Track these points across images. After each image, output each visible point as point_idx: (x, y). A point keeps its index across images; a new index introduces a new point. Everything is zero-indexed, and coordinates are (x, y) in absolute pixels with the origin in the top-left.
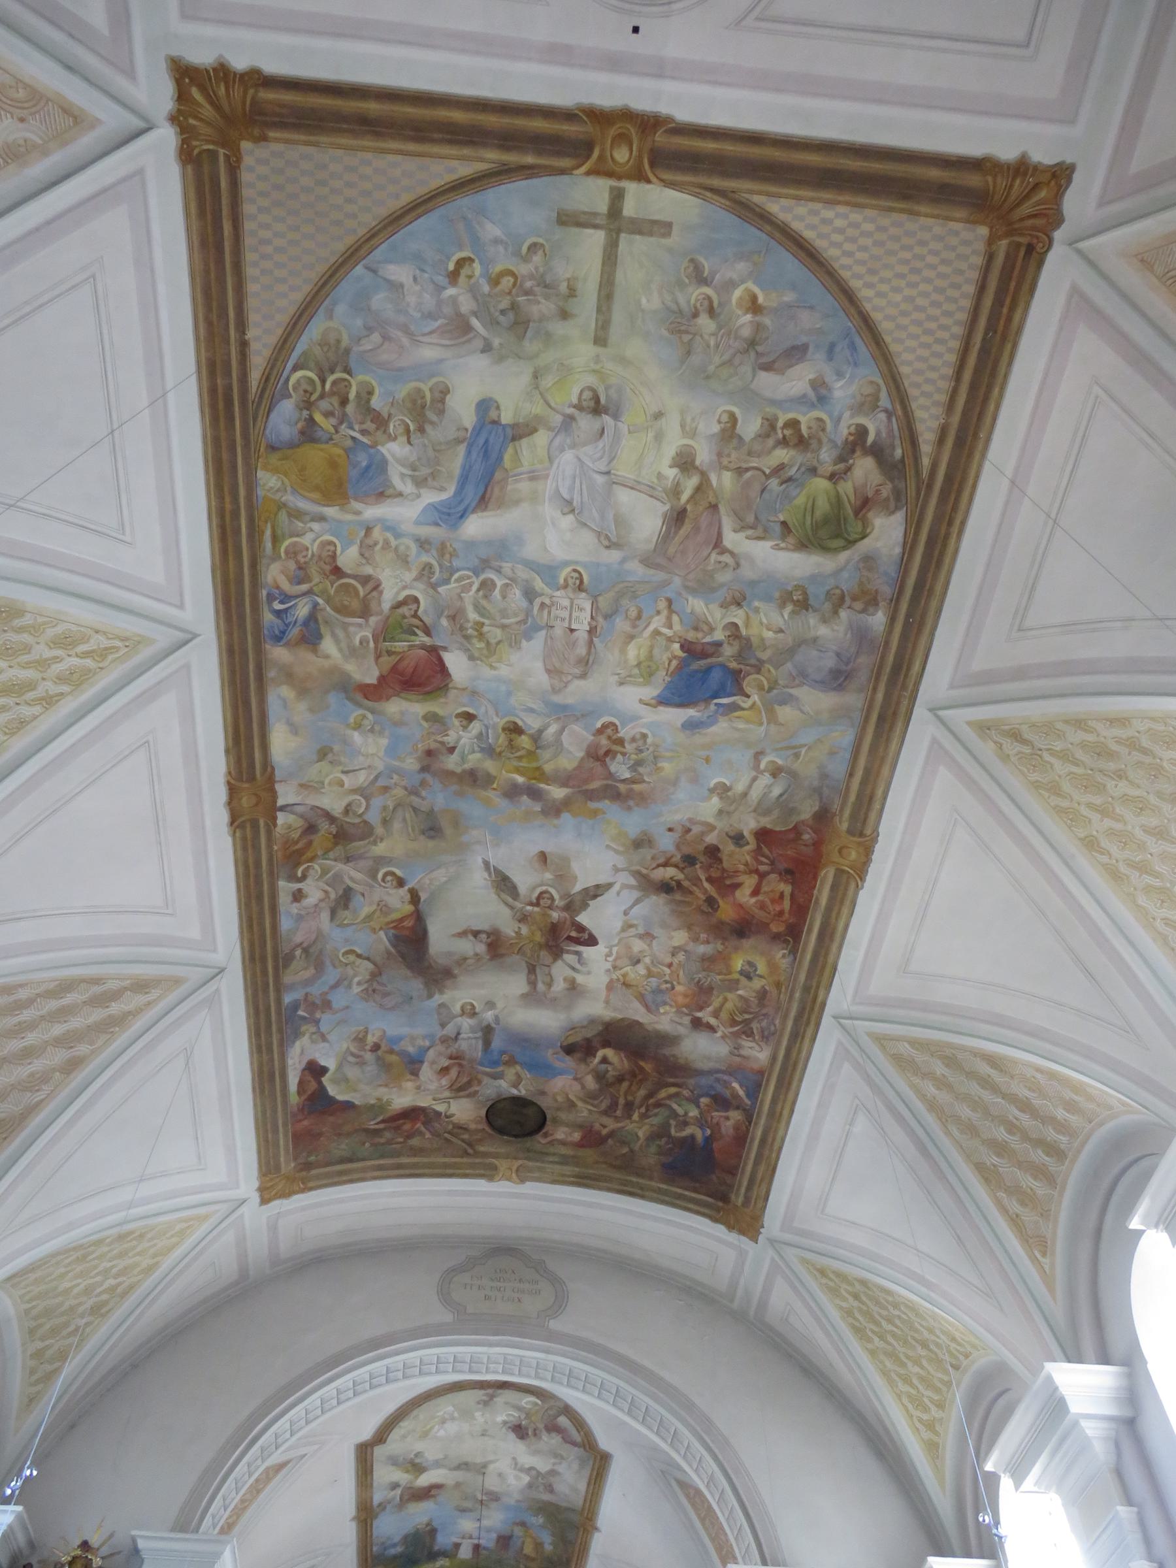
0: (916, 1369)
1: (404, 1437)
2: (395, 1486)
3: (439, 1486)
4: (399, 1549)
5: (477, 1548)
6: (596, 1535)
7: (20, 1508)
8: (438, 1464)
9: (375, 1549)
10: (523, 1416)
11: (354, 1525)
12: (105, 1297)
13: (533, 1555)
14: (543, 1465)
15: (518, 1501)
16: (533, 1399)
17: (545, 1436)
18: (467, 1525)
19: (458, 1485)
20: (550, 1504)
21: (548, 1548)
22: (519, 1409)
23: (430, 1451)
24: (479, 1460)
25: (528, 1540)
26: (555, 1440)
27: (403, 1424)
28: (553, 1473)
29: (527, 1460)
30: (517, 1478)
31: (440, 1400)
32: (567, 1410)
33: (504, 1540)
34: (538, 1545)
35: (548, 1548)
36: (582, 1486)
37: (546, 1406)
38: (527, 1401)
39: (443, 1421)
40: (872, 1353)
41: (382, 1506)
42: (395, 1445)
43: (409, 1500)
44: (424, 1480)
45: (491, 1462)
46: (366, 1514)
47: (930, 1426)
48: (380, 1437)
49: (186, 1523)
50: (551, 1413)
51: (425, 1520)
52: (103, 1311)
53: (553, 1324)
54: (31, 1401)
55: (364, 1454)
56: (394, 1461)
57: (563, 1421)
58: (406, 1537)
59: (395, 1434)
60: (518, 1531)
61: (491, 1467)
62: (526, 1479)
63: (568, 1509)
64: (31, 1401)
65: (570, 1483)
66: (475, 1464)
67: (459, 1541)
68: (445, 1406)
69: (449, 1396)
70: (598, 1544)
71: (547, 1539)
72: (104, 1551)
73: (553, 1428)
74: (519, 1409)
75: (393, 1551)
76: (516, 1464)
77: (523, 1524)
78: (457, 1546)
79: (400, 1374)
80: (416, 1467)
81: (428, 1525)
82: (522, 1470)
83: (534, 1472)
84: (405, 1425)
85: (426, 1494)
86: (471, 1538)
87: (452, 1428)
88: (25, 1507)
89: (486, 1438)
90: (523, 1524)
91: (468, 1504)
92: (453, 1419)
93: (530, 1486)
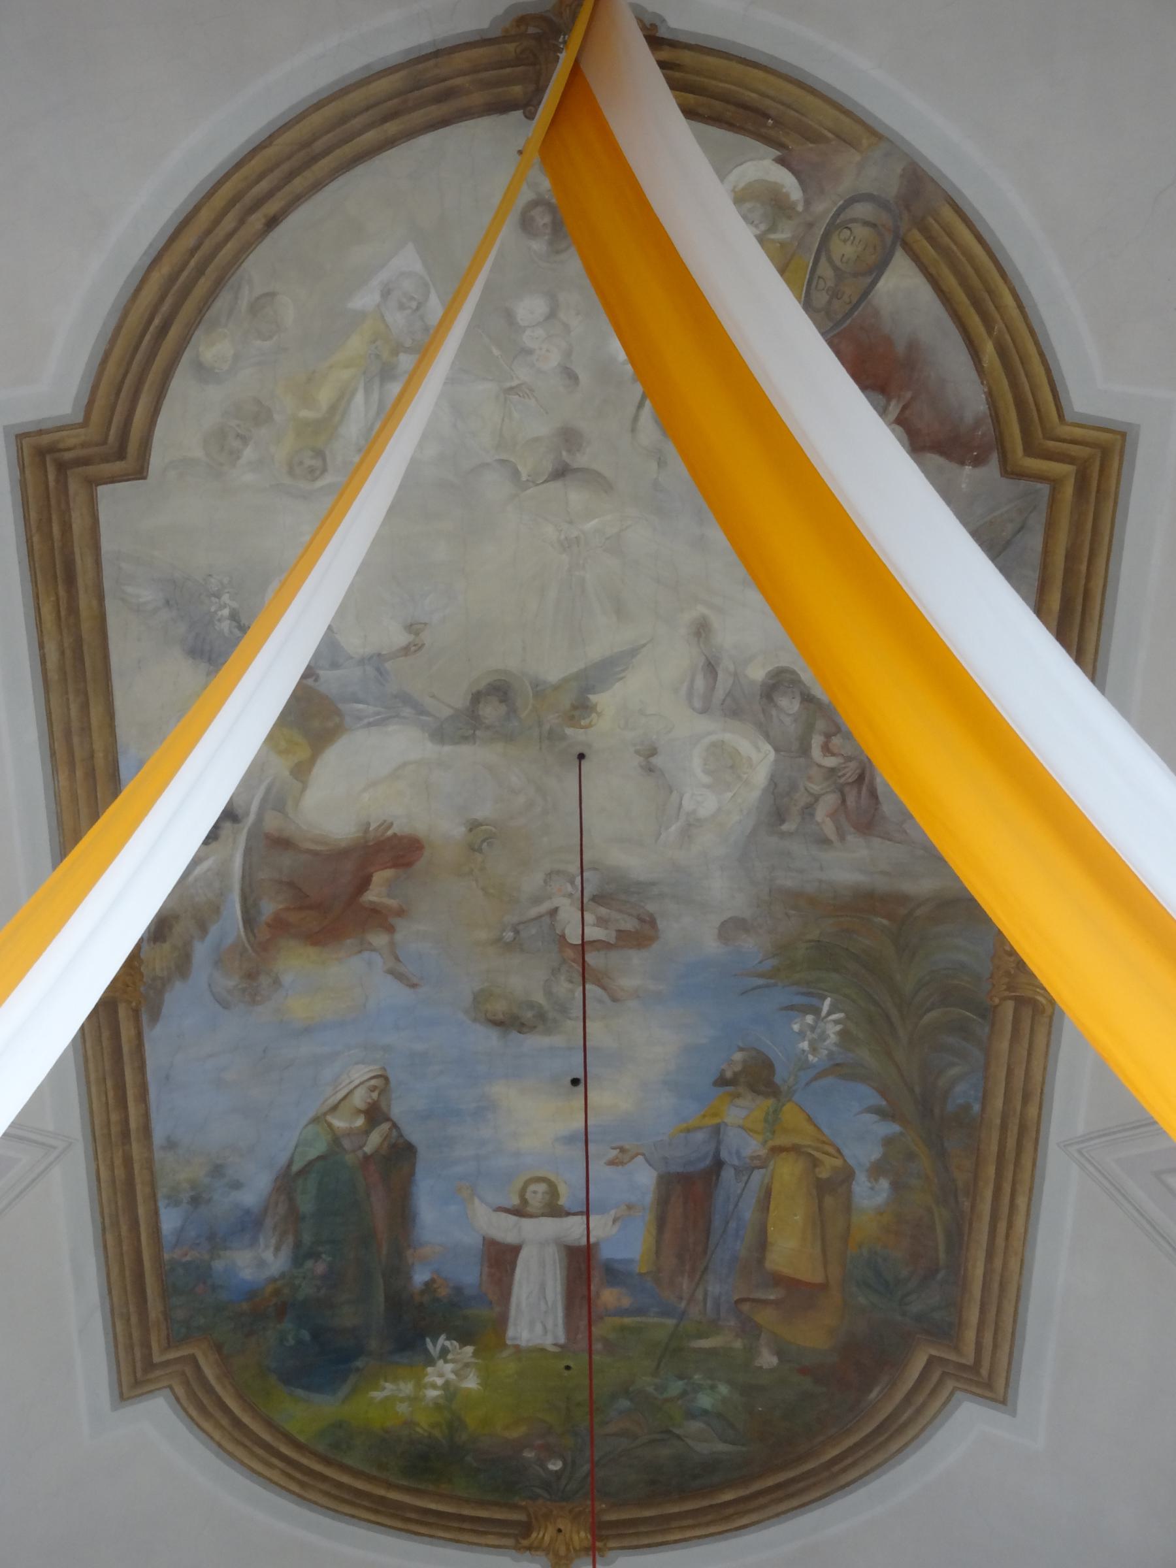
1: (225, 443)
4: (259, 1263)
5: (581, 1263)
9: (170, 1220)
13: (808, 1271)
15: (731, 928)
18: (532, 1123)
19: (481, 838)
20: (866, 904)
21: (870, 1195)
24: (554, 667)
25: (787, 1172)
27: (214, 347)
30: (725, 764)
31: (361, 193)
33: (691, 1194)
34: (830, 1188)
35: (870, 1195)
37: (825, 207)
45: (606, 671)
50: (844, 249)
58: (288, 1182)
59: (184, 423)
61: (605, 700)
66: (540, 690)
67: (506, 1229)
69: (398, 163)
76: (711, 668)
78: (501, 1259)
81: (374, 1114)
82: (734, 710)
83: (789, 704)
86: (554, 1210)
89: (576, 496)
91: (526, 980)
93: (779, 808)
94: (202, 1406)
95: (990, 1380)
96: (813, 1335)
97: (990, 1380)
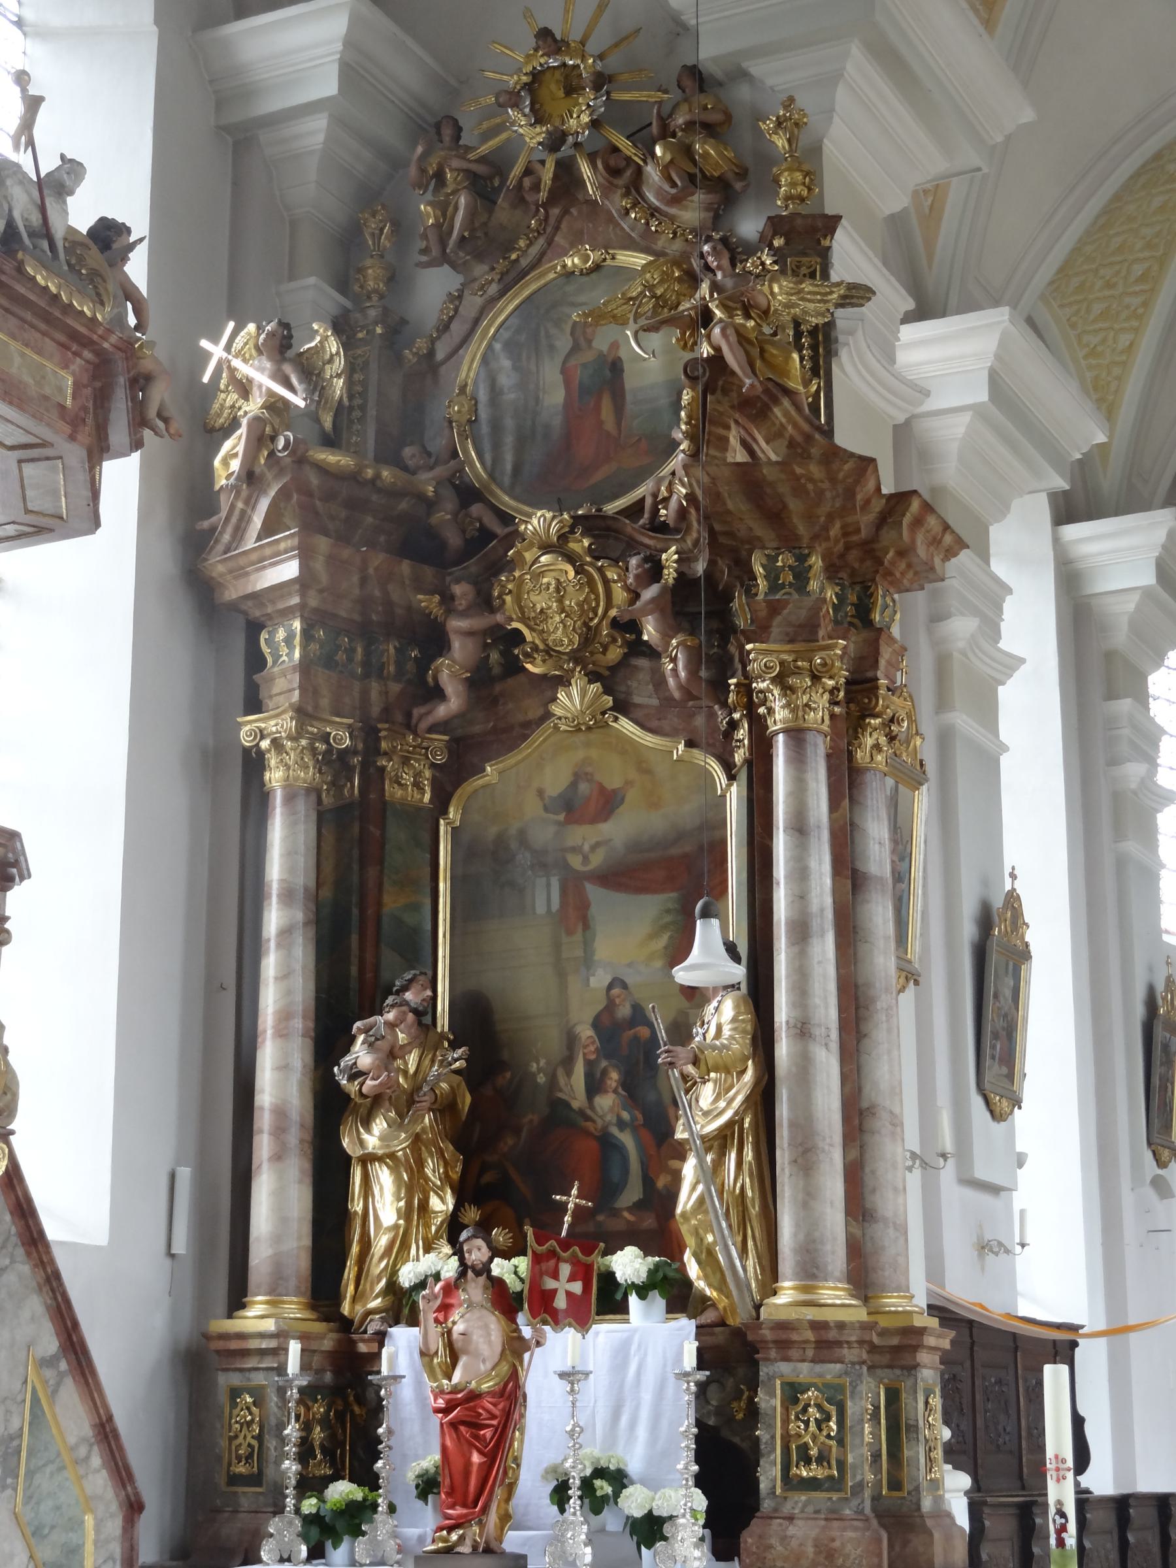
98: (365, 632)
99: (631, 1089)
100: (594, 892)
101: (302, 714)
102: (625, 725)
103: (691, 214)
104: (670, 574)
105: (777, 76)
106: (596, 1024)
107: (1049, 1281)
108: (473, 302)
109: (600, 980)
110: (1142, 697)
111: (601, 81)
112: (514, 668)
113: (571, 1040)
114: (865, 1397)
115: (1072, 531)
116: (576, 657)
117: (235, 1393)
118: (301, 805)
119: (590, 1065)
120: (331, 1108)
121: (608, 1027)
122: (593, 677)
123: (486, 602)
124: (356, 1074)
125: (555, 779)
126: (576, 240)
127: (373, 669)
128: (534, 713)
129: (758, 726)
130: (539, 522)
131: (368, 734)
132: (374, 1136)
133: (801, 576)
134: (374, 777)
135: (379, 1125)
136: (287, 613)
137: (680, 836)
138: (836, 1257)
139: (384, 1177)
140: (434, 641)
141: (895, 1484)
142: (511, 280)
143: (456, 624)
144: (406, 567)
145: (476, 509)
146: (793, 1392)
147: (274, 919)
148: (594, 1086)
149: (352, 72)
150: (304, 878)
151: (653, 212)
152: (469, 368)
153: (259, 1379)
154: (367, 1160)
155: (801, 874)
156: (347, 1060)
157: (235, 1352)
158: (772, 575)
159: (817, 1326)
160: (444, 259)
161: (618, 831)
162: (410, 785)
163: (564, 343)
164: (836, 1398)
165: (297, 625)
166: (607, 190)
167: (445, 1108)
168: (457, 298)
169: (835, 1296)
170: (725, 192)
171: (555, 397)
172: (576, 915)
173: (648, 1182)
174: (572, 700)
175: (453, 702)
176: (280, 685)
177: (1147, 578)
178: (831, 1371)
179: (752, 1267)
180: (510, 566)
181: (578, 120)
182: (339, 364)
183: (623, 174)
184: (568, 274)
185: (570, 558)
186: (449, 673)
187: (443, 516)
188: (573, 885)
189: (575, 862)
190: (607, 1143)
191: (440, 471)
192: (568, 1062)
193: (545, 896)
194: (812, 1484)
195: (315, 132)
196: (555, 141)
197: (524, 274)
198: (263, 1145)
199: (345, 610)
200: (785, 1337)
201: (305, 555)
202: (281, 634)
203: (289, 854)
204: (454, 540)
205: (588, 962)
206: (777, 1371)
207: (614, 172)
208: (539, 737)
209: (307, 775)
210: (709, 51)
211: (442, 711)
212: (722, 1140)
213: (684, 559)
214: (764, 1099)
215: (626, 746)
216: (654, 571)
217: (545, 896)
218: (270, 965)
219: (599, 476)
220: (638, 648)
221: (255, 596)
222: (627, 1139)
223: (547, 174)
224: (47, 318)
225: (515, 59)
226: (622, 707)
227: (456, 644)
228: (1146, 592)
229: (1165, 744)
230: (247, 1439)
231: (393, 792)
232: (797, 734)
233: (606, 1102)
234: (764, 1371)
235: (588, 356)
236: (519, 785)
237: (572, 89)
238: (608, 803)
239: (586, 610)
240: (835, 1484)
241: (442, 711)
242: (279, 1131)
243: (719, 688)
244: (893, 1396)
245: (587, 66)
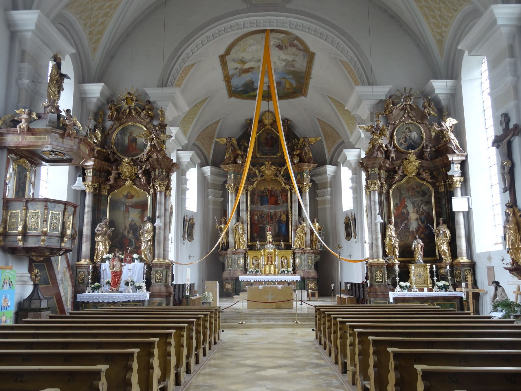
0: (439, 13)
2: (236, 69)
3: (253, 68)
4: (242, 89)
6: (311, 80)
7: (103, 84)
8: (250, 60)
10: (280, 42)
11: (224, 82)
12: (108, 10)
13: (289, 88)
14: (290, 58)
16: (284, 35)
17: (290, 48)
22: (279, 39)
23: (247, 56)
26: (294, 49)
28: (294, 60)
29: (284, 57)
31: (248, 38)
32: (297, 38)
34: (291, 84)
36: (305, 64)
38: (282, 36)
39: (250, 46)
40: (421, 7)
41: (233, 76)
42: (233, 54)
43: (242, 73)
44: (246, 66)
46: (228, 79)
47: (441, 34)
48: (228, 52)
49: (163, 84)
51: (249, 79)
52: (109, 15)
53: (288, 6)
54: (94, 49)
55: (223, 59)
56: (234, 60)
57: (296, 42)
58: (243, 85)
59: (233, 51)
60: (283, 81)
62: (284, 63)
63: (300, 72)
64: (94, 49)
65: (300, 64)
68: (250, 40)
69: (251, 36)
70: (312, 83)
71: (294, 83)
72: (136, 95)
73: (292, 45)
74: (279, 39)
75: (239, 89)
77: (284, 78)
79: (230, 30)
80: (243, 62)
82: (282, 60)
84: (236, 48)
85: (248, 71)
87: (254, 48)
88: (105, 84)
90: (284, 78)
92: (254, 45)
93: (286, 65)
94: (236, 97)
95: (305, 95)
96: (290, 91)
97: (305, 95)
98: (100, 171)
99: (134, 233)
100: (130, 208)
101: (92, 182)
102: (135, 187)
103: (148, 120)
104: (143, 169)
105: (159, 104)
106: (129, 225)
107: (171, 257)
108: (115, 126)
109: (130, 219)
110: (185, 175)
111: (136, 101)
112: (120, 177)
113: (126, 227)
114: (164, 273)
115: (179, 152)
116: (129, 177)
117: (80, 272)
118: (91, 194)
119: (128, 231)
120: (93, 234)
121: (131, 226)
122: (131, 180)
123: (117, 169)
124: (98, 231)
125: (125, 193)
126: (131, 121)
127: (100, 176)
128: (122, 184)
129: (155, 190)
130: (126, 160)
131: (100, 185)
132: (100, 238)
133: (162, 172)
134: (100, 191)
135: (100, 237)
136: (90, 168)
137: (142, 202)
138: (162, 256)
139: (101, 244)
140: (109, 173)
141: (166, 282)
142: (121, 124)
143: (113, 172)
144: (107, 163)
145: (115, 156)
146: (157, 272)
147: (86, 210)
148: (129, 233)
149: (102, 93)
150: (91, 204)
151: (142, 119)
152: (114, 136)
153: (84, 270)
154: (98, 242)
155: (160, 209)
156: (97, 228)
157: (81, 266)
158: (159, 172)
159: (160, 264)
160: (111, 120)
161: (134, 200)
162: (105, 192)
163: (128, 134)
164: (162, 272)
165: (92, 170)
166: (136, 114)
167: (109, 235)
168: (113, 125)
169: (162, 260)
170: (152, 118)
171: (127, 141)
172: (127, 211)
173: (135, 245)
174: (128, 183)
175: (112, 182)
176: (88, 178)
177: (189, 160)
178: (161, 269)
179: (151, 256)
180: (121, 165)
181: (133, 105)
182: (100, 136)
183: (137, 112)
184: (129, 125)
185: (130, 165)
186: (111, 178)
187: (111, 156)
188: (127, 207)
189: (127, 204)
190: (130, 240)
191: (111, 150)
192: (125, 230)
193: (123, 208)
194: (158, 282)
195: (95, 100)
196: (129, 108)
197: (123, 124)
198: (84, 239)
199: (98, 168)
200: (156, 265)
201: (94, 162)
202: (89, 171)
203: (89, 201)
204: (112, 160)
205: (129, 217)
206: (154, 270)
207: (137, 113)
208: (123, 187)
209: (92, 190)
210: (151, 100)
211: (110, 183)
212: (148, 241)
213: (146, 167)
214: (154, 237)
215: (135, 189)
216: (141, 168)
217: (123, 208)
218: (86, 216)
219: (133, 153)
220: (138, 177)
221: (86, 166)
222: (133, 240)
223: (128, 111)
224: (87, 144)
225: (124, 95)
226: (135, 184)
227: (113, 174)
228: (189, 162)
229: (188, 182)
230: (81, 278)
231: (103, 193)
232: (160, 192)
233: (130, 235)
234: (153, 269)
235: (132, 137)
236: (120, 193)
237: (132, 100)
238: (132, 197)
239: (131, 172)
240: (161, 282)
241: (110, 183)
242: (86, 238)
243: (149, 184)
244: (166, 272)
245: (135, 98)
